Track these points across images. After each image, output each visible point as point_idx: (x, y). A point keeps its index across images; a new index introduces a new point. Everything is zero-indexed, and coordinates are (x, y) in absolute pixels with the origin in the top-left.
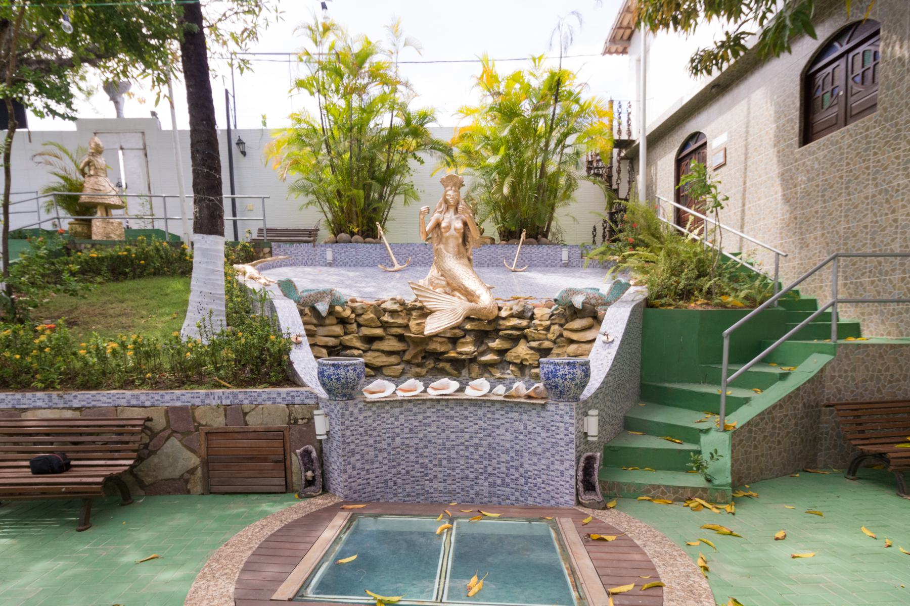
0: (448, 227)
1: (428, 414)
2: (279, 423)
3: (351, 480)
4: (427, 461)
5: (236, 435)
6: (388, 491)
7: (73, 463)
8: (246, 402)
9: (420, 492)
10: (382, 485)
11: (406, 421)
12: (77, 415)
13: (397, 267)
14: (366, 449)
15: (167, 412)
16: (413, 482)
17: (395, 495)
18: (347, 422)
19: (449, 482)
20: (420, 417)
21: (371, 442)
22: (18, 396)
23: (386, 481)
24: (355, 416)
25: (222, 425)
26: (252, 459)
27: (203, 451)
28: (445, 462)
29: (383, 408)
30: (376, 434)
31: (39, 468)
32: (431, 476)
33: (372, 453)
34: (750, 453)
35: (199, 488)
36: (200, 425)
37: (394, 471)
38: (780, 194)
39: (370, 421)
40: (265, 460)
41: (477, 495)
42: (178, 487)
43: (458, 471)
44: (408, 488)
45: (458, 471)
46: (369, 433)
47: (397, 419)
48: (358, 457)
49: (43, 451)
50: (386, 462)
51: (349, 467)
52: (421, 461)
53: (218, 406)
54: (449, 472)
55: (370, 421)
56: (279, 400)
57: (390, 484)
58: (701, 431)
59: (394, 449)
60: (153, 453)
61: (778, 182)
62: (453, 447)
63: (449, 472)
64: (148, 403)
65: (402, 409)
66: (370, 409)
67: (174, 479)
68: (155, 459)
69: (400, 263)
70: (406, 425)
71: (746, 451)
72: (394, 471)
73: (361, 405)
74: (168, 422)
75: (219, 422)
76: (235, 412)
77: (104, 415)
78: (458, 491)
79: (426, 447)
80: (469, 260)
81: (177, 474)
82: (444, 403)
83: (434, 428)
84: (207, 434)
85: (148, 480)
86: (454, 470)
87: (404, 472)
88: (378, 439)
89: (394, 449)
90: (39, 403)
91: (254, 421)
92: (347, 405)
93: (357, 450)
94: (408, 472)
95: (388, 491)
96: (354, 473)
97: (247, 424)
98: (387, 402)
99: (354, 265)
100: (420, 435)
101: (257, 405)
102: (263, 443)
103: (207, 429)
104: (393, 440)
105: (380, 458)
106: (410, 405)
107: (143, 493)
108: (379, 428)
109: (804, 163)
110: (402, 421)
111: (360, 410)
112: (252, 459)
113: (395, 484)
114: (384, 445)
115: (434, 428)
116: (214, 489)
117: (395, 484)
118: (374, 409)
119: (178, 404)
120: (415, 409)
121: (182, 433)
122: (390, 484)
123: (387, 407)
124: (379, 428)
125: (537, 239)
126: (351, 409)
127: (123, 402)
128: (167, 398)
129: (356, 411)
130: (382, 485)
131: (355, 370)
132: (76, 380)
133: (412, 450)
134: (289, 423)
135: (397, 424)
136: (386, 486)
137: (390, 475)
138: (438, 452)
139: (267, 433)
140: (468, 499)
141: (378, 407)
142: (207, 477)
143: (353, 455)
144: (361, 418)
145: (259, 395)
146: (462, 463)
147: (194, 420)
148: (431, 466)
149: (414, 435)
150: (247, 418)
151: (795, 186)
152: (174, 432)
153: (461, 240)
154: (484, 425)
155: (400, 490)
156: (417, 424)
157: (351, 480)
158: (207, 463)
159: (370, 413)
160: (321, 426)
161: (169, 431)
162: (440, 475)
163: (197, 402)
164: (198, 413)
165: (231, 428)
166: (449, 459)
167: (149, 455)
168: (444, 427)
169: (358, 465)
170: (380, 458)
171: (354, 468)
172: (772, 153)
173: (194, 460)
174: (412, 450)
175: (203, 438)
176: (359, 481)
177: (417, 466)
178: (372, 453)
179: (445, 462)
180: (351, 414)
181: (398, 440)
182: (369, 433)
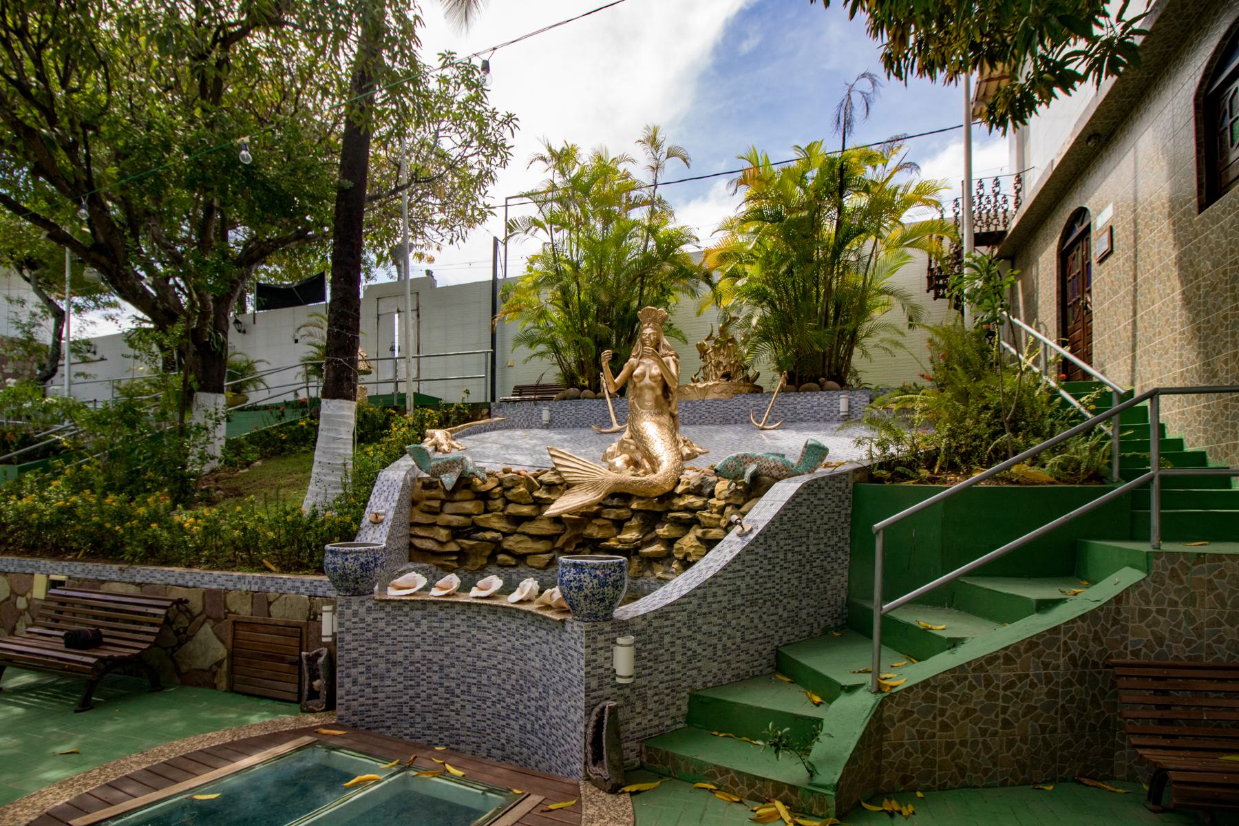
0: (643, 375)
1: (457, 622)
2: (300, 618)
3: (350, 697)
4: (453, 685)
5: (259, 628)
6: (403, 717)
7: (105, 640)
8: (272, 589)
9: (444, 725)
10: (395, 709)
11: (430, 628)
12: (132, 590)
13: (616, 427)
14: (375, 660)
15: (204, 594)
16: (435, 711)
17: (412, 725)
18: (347, 623)
19: (479, 718)
20: (447, 625)
21: (382, 651)
22: (100, 566)
23: (401, 704)
24: (361, 616)
25: (248, 616)
26: (271, 657)
27: (229, 642)
28: (474, 689)
29: (400, 609)
30: (390, 642)
31: (74, 641)
32: (458, 706)
33: (382, 666)
34: (934, 736)
35: (223, 684)
36: (230, 612)
37: (411, 692)
38: (1178, 291)
39: (382, 624)
40: (282, 660)
41: (508, 741)
42: (202, 680)
43: (489, 704)
44: (429, 718)
45: (489, 704)
46: (380, 639)
47: (418, 624)
48: (362, 669)
49: (83, 625)
50: (401, 679)
51: (346, 680)
52: (446, 684)
53: (247, 592)
54: (479, 703)
55: (382, 624)
56: (302, 590)
57: (406, 709)
58: (843, 687)
59: (412, 663)
60: (189, 638)
61: (1175, 272)
62: (484, 669)
63: (479, 703)
64: (191, 584)
65: (425, 613)
66: (382, 609)
67: (203, 670)
68: (190, 646)
69: (619, 423)
70: (429, 633)
71: (921, 734)
72: (411, 692)
73: (369, 603)
74: (204, 605)
75: (245, 610)
76: (262, 601)
77: (157, 593)
78: (489, 731)
79: (453, 665)
80: (672, 416)
81: (206, 665)
82: (476, 609)
83: (463, 641)
84: (235, 623)
85: (184, 668)
86: (484, 701)
87: (423, 695)
88: (391, 648)
89: (412, 663)
90: (114, 576)
91: (278, 613)
92: (349, 602)
93: (361, 659)
94: (429, 697)
95: (403, 717)
96: (355, 689)
97: (270, 616)
98: (406, 602)
99: (574, 427)
100: (447, 649)
101: (281, 594)
102: (281, 640)
103: (232, 617)
104: (412, 651)
105: (393, 674)
106: (435, 608)
107: (179, 681)
108: (393, 634)
109: (1206, 237)
110: (424, 628)
111: (369, 610)
112: (271, 657)
113: (412, 710)
114: (399, 656)
115: (463, 641)
116: (237, 687)
117: (412, 710)
118: (388, 609)
119: (215, 587)
120: (441, 614)
121: (215, 620)
122: (406, 709)
123: (406, 609)
124: (393, 634)
125: (818, 383)
126: (354, 607)
127: (172, 580)
128: (206, 578)
129: (362, 610)
130: (395, 709)
131: (356, 559)
132: (154, 554)
133: (436, 668)
134: (309, 619)
135: (418, 631)
136: (400, 712)
137: (405, 698)
138: (467, 674)
139: (287, 628)
140: (499, 745)
141: (394, 608)
142: (231, 672)
143: (355, 666)
144: (369, 619)
145: (285, 581)
146: (494, 693)
147: (226, 607)
148: (458, 691)
149: (438, 648)
150: (271, 608)
151: (1197, 278)
152: (208, 617)
153: (659, 392)
154: (517, 643)
155: (418, 720)
156: (443, 634)
157: (350, 697)
158: (232, 656)
159: (382, 615)
160: (328, 624)
161: (204, 616)
162: (469, 707)
163: (230, 585)
164: (229, 598)
165: (255, 618)
166: (479, 685)
167: (186, 641)
168: (474, 641)
169: (361, 679)
170: (393, 674)
171: (355, 682)
172: (1165, 225)
173: (220, 651)
174: (436, 668)
175: (230, 627)
176: (361, 700)
177: (441, 690)
178: (382, 666)
179: (474, 689)
180: (355, 614)
181: (418, 652)
182: (380, 639)
